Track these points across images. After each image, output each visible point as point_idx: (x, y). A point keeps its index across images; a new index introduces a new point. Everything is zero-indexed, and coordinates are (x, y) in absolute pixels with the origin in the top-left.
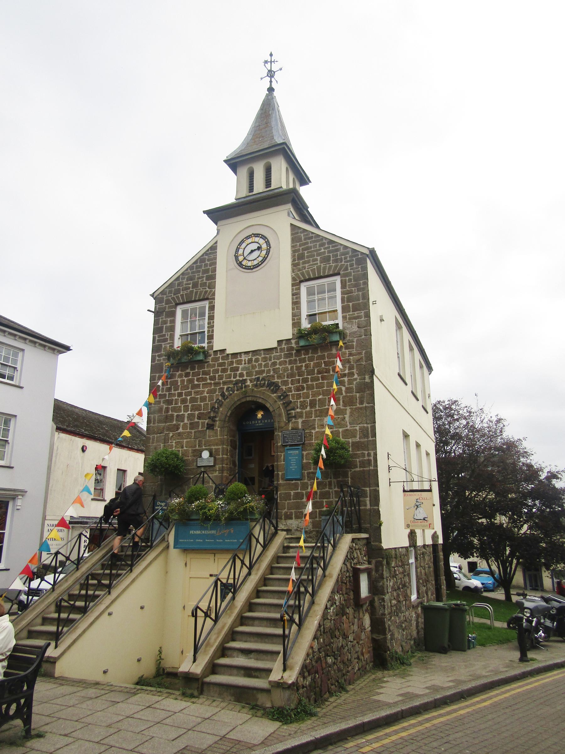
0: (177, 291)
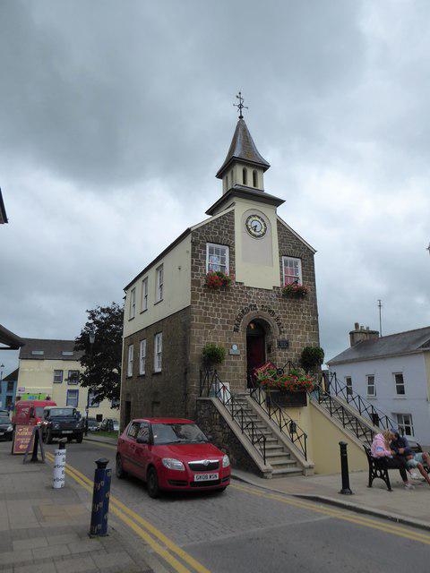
0: (208, 233)
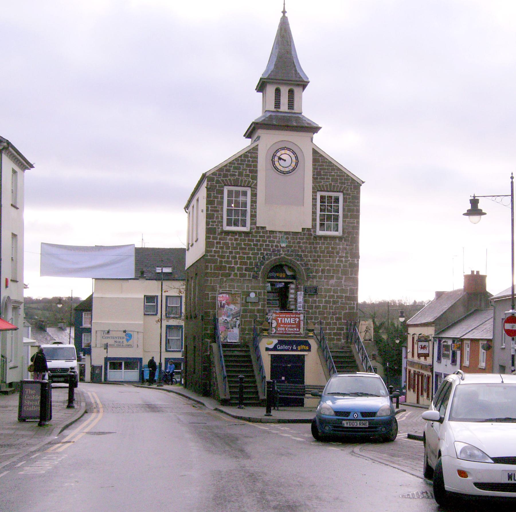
0: (226, 176)
